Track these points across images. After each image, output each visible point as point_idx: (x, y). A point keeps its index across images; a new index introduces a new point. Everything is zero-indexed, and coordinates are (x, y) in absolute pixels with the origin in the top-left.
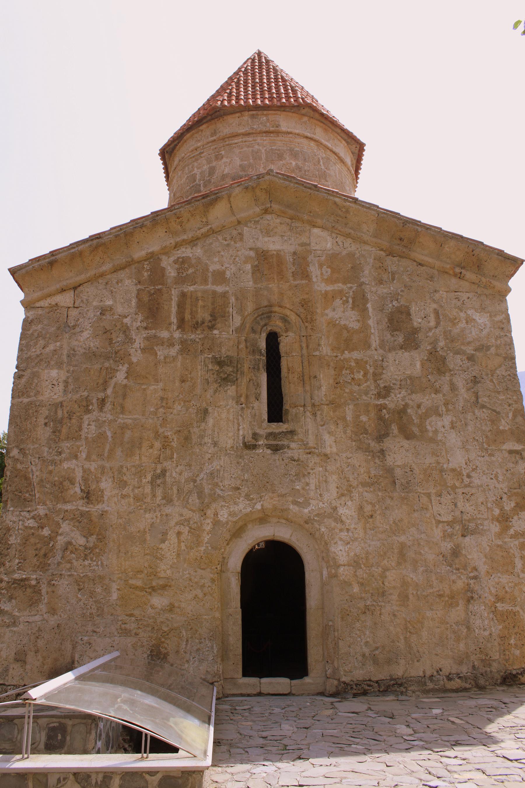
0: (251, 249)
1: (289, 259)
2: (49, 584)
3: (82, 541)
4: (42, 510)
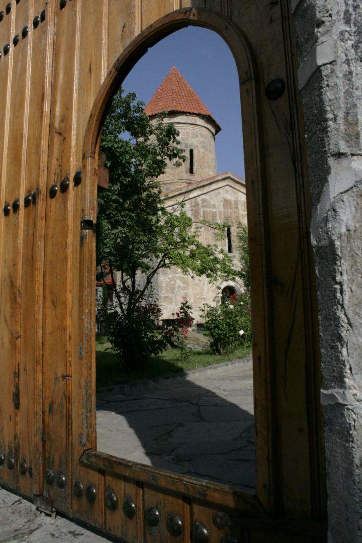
0: (222, 198)
1: (233, 202)
2: (175, 297)
3: (182, 285)
4: (170, 276)
